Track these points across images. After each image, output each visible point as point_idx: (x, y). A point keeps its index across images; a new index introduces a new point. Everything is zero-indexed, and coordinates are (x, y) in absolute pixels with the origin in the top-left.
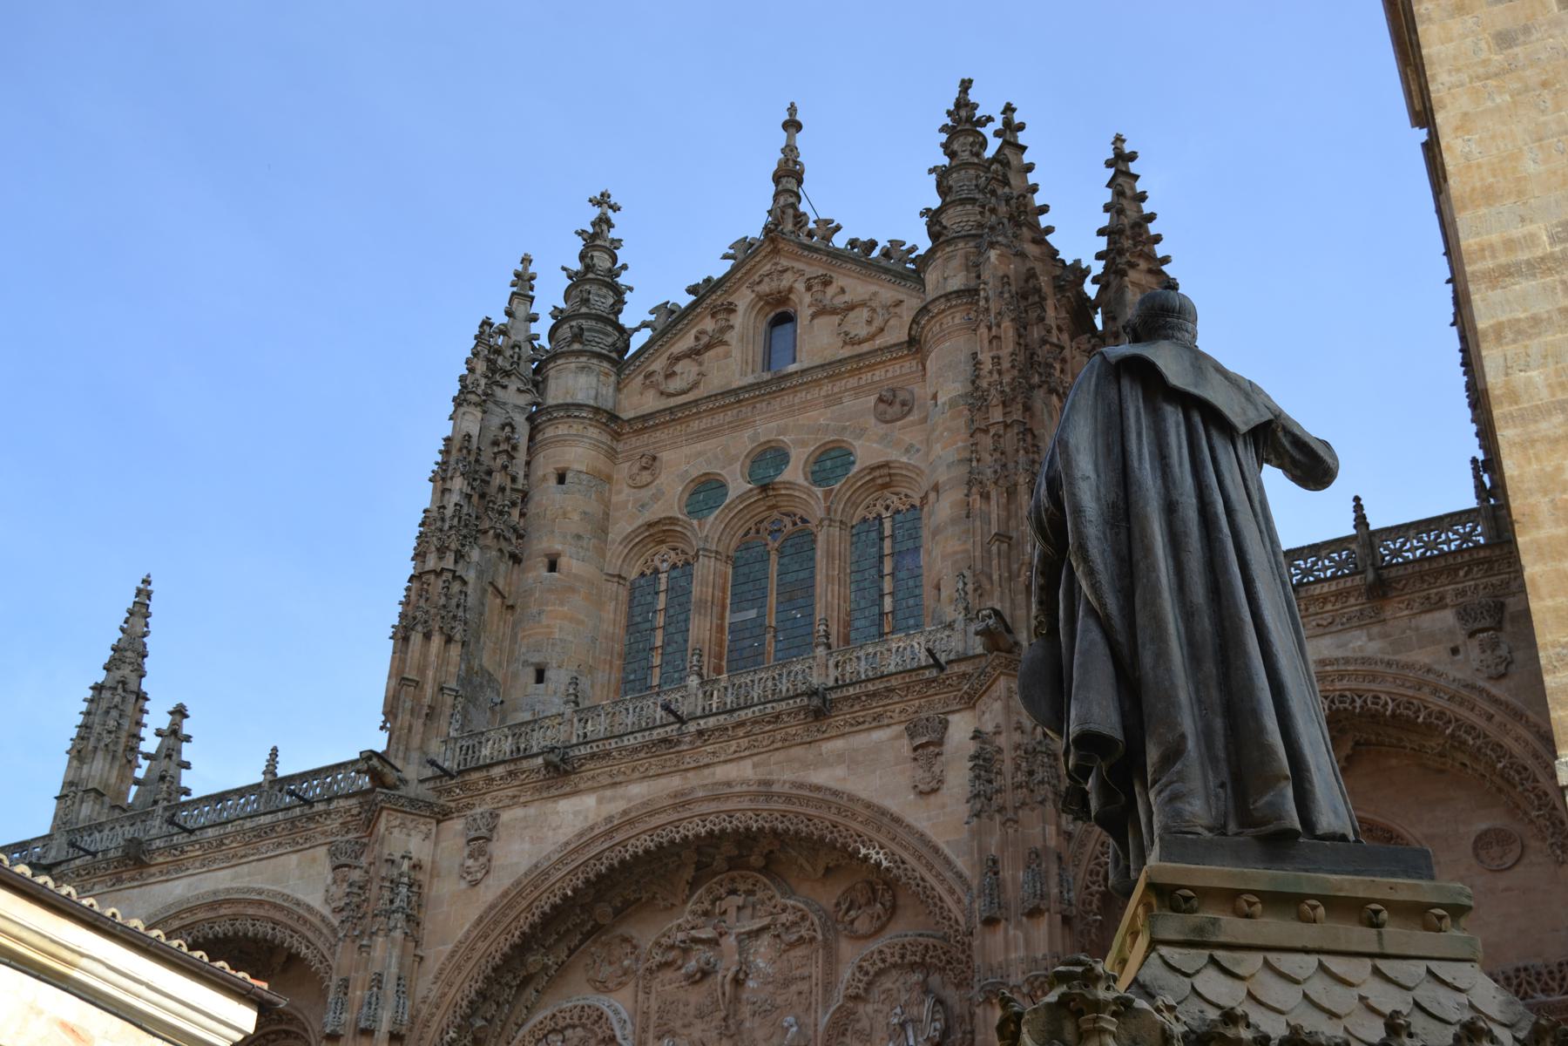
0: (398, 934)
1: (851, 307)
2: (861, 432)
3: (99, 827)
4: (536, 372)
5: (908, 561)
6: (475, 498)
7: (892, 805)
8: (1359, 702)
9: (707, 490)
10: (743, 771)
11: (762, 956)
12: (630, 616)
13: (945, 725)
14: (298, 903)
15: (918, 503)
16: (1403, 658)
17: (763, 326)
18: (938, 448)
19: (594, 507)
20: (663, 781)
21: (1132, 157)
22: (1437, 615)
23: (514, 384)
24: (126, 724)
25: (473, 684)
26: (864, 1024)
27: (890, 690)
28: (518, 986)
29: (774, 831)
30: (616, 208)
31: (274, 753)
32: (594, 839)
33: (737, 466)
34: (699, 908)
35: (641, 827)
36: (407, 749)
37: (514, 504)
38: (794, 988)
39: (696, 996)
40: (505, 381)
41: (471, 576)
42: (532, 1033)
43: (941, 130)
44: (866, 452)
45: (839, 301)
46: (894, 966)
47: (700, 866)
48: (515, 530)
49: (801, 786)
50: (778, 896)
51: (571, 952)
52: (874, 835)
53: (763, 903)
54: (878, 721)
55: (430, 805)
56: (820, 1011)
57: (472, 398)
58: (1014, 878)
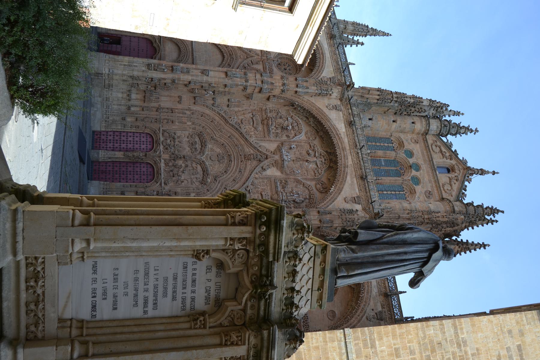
0: (317, 92)
1: (451, 186)
2: (423, 187)
3: (338, 29)
4: (437, 117)
5: (394, 197)
6: (409, 104)
7: (343, 193)
8: (362, 289)
9: (410, 154)
10: (350, 162)
11: (312, 166)
12: (383, 138)
13: (359, 204)
14: (323, 71)
15: (407, 199)
16: (372, 299)
17: (447, 166)
19: (407, 130)
20: (348, 145)
21: (485, 248)
22: (381, 307)
23: (434, 112)
24: (360, 33)
25: (368, 105)
26: (299, 186)
27: (367, 193)
29: (338, 168)
30: (475, 134)
31: (354, 64)
32: (336, 132)
33: (416, 161)
34: (322, 153)
35: (338, 141)
36: (355, 92)
37: (407, 113)
39: (304, 153)
40: (435, 110)
41: (392, 104)
42: (297, 119)
43: (492, 206)
44: (418, 189)
45: (453, 183)
46: (310, 193)
47: (330, 153)
48: (402, 113)
49: (347, 174)
51: (313, 127)
52: (337, 189)
54: (360, 190)
57: (431, 103)
58: (327, 217)
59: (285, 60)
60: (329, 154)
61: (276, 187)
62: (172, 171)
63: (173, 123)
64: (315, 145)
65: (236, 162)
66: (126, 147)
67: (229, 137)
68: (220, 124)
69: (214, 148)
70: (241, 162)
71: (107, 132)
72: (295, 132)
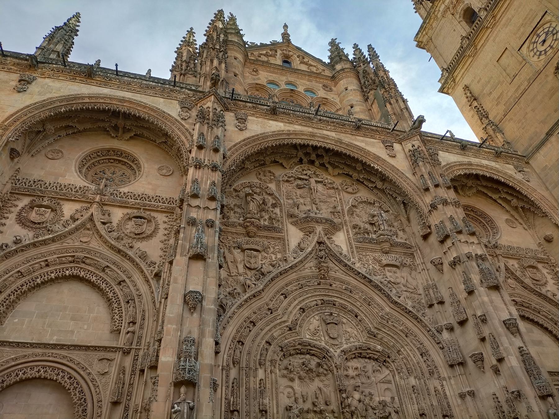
11: (320, 187)
14: (164, 112)
18: (352, 97)
33: (284, 83)
39: (299, 192)
46: (365, 202)
50: (324, 175)
51: (255, 167)
54: (372, 137)
55: (225, 104)
59: (90, 172)
60: (301, 161)
61: (371, 241)
67: (286, 297)
68: (259, 309)
69: (312, 327)
70: (331, 285)
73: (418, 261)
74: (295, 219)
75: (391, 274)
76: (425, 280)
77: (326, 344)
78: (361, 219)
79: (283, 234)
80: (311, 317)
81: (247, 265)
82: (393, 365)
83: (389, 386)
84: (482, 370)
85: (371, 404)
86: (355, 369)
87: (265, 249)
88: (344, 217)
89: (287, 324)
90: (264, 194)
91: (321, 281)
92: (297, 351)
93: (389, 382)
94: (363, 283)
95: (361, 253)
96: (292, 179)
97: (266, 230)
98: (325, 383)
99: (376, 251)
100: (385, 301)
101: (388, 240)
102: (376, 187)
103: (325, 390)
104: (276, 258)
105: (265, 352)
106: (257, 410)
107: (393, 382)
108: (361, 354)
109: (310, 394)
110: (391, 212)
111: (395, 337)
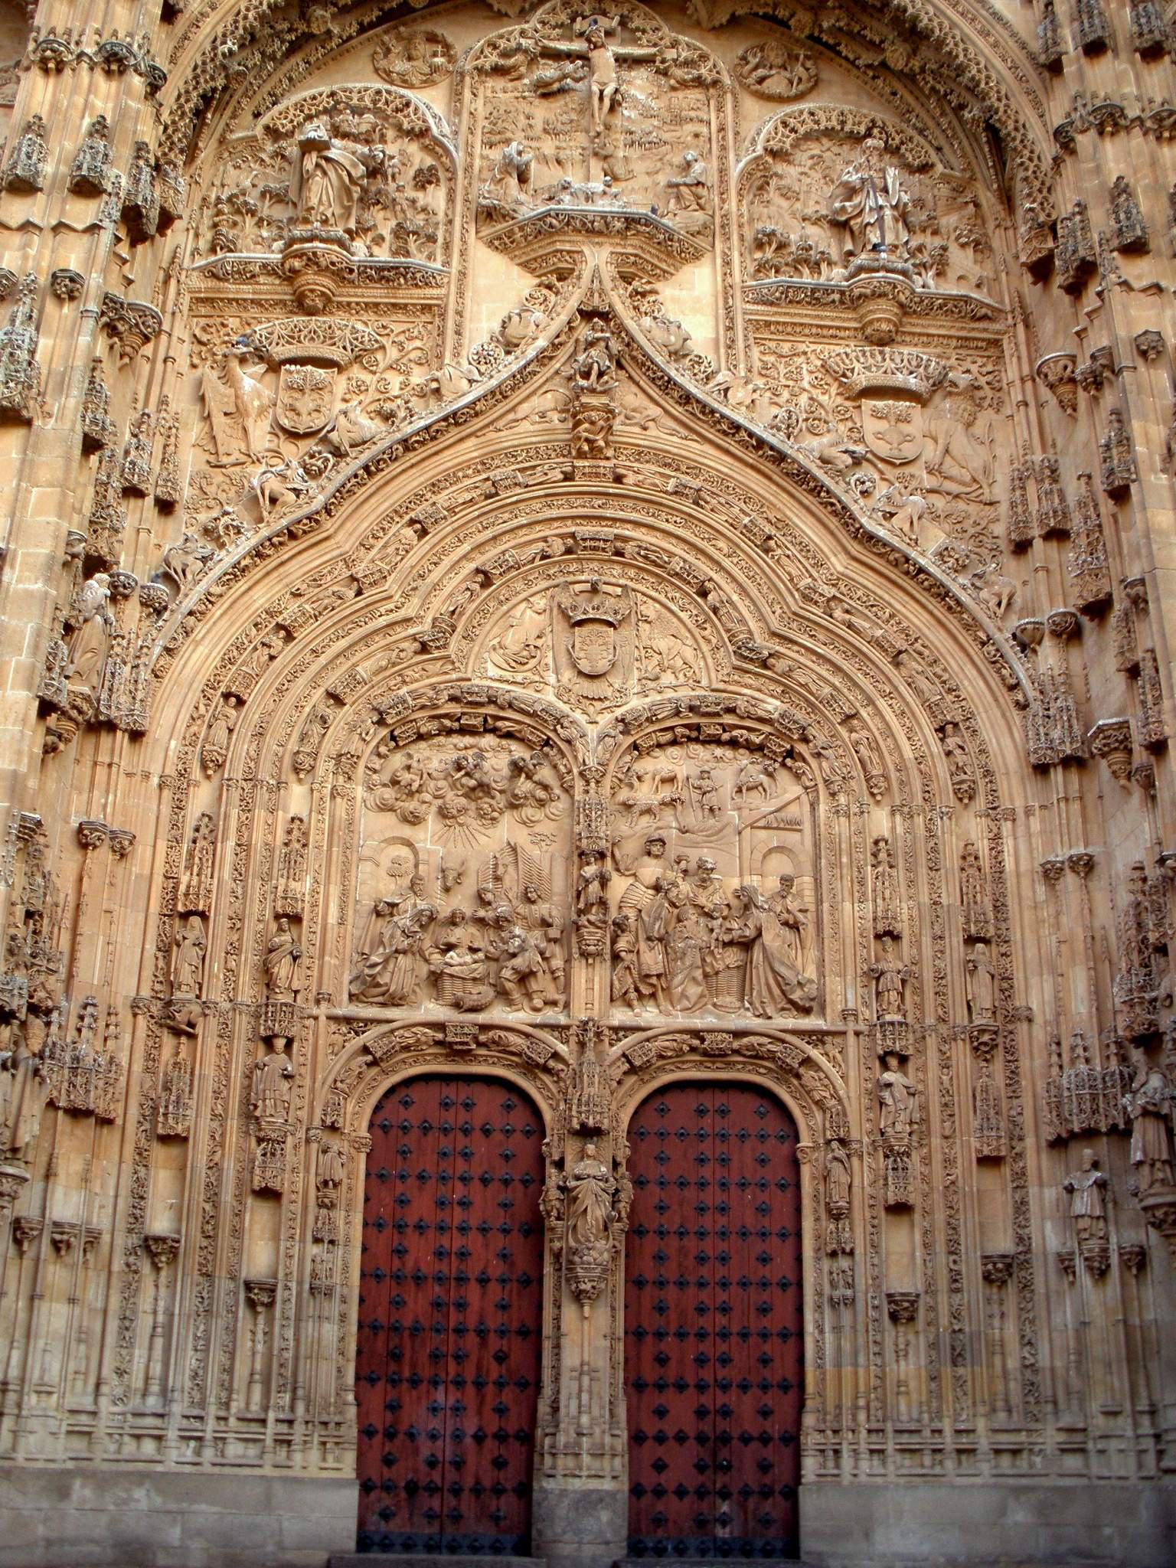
11: (640, 85)
28: (291, 42)
38: (690, 128)
39: (543, 112)
46: (828, 133)
50: (666, 30)
51: (363, 29)
53: (644, 31)
56: (732, 157)
61: (816, 297)
62: (703, 960)
63: (296, 919)
64: (495, 47)
65: (621, 514)
66: (495, 1291)
67: (423, 533)
68: (316, 582)
69: (513, 640)
70: (618, 479)
71: (366, 1432)
72: (390, 134)
73: (1012, 371)
74: (501, 227)
75: (882, 426)
76: (1020, 442)
77: (559, 696)
78: (798, 205)
79: (443, 291)
80: (515, 600)
81: (286, 423)
82: (817, 772)
83: (791, 838)
84: (1123, 782)
85: (702, 900)
86: (663, 781)
87: (361, 356)
88: (723, 201)
89: (411, 631)
90: (390, 134)
91: (579, 463)
92: (447, 722)
93: (793, 826)
94: (752, 467)
95: (772, 345)
96: (519, 58)
97: (370, 278)
98: (538, 829)
99: (842, 334)
100: (832, 533)
101: (888, 288)
102: (884, 64)
103: (535, 852)
104: (404, 385)
105: (317, 729)
106: (268, 914)
107: (807, 827)
108: (698, 728)
109: (473, 865)
110: (940, 168)
111: (845, 665)
